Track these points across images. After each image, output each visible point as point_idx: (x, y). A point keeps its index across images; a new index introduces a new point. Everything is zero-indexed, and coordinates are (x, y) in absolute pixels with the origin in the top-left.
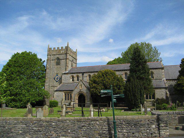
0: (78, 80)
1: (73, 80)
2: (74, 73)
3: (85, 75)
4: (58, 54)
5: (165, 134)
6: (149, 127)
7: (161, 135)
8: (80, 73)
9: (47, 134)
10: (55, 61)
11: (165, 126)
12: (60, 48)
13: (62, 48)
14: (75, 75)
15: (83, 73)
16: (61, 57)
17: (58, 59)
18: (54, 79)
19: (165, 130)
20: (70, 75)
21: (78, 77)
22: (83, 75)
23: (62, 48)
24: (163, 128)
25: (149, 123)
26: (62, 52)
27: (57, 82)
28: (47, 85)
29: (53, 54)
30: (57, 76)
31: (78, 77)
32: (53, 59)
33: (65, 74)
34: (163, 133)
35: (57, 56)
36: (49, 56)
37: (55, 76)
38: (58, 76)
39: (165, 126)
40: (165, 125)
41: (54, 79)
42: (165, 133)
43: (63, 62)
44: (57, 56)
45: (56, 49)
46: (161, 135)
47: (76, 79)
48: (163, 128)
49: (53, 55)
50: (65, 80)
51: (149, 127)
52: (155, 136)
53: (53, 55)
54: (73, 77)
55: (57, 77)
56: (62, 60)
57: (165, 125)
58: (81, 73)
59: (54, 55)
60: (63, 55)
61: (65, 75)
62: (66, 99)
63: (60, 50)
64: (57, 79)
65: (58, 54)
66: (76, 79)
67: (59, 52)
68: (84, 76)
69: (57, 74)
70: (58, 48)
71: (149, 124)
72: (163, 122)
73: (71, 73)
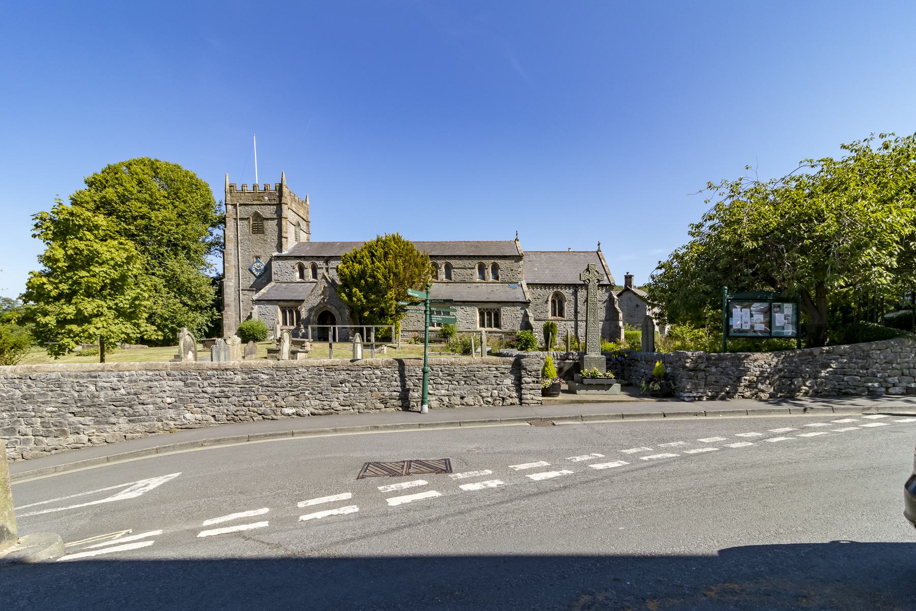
0: (315, 275)
1: (302, 276)
4: (255, 203)
5: (532, 399)
6: (499, 384)
7: (523, 401)
9: (246, 403)
11: (534, 382)
12: (262, 188)
14: (307, 264)
15: (327, 259)
17: (257, 216)
19: (532, 392)
20: (294, 263)
24: (528, 386)
25: (499, 375)
26: (267, 198)
28: (229, 286)
31: (314, 269)
34: (529, 396)
38: (259, 262)
39: (534, 382)
40: (534, 379)
42: (534, 397)
43: (271, 226)
46: (523, 401)
47: (309, 272)
48: (528, 386)
49: (241, 205)
51: (499, 384)
52: (511, 404)
53: (241, 205)
54: (301, 269)
55: (258, 264)
57: (534, 379)
60: (272, 207)
61: (280, 262)
62: (285, 323)
66: (309, 272)
69: (257, 257)
71: (498, 377)
72: (531, 372)
73: (296, 257)
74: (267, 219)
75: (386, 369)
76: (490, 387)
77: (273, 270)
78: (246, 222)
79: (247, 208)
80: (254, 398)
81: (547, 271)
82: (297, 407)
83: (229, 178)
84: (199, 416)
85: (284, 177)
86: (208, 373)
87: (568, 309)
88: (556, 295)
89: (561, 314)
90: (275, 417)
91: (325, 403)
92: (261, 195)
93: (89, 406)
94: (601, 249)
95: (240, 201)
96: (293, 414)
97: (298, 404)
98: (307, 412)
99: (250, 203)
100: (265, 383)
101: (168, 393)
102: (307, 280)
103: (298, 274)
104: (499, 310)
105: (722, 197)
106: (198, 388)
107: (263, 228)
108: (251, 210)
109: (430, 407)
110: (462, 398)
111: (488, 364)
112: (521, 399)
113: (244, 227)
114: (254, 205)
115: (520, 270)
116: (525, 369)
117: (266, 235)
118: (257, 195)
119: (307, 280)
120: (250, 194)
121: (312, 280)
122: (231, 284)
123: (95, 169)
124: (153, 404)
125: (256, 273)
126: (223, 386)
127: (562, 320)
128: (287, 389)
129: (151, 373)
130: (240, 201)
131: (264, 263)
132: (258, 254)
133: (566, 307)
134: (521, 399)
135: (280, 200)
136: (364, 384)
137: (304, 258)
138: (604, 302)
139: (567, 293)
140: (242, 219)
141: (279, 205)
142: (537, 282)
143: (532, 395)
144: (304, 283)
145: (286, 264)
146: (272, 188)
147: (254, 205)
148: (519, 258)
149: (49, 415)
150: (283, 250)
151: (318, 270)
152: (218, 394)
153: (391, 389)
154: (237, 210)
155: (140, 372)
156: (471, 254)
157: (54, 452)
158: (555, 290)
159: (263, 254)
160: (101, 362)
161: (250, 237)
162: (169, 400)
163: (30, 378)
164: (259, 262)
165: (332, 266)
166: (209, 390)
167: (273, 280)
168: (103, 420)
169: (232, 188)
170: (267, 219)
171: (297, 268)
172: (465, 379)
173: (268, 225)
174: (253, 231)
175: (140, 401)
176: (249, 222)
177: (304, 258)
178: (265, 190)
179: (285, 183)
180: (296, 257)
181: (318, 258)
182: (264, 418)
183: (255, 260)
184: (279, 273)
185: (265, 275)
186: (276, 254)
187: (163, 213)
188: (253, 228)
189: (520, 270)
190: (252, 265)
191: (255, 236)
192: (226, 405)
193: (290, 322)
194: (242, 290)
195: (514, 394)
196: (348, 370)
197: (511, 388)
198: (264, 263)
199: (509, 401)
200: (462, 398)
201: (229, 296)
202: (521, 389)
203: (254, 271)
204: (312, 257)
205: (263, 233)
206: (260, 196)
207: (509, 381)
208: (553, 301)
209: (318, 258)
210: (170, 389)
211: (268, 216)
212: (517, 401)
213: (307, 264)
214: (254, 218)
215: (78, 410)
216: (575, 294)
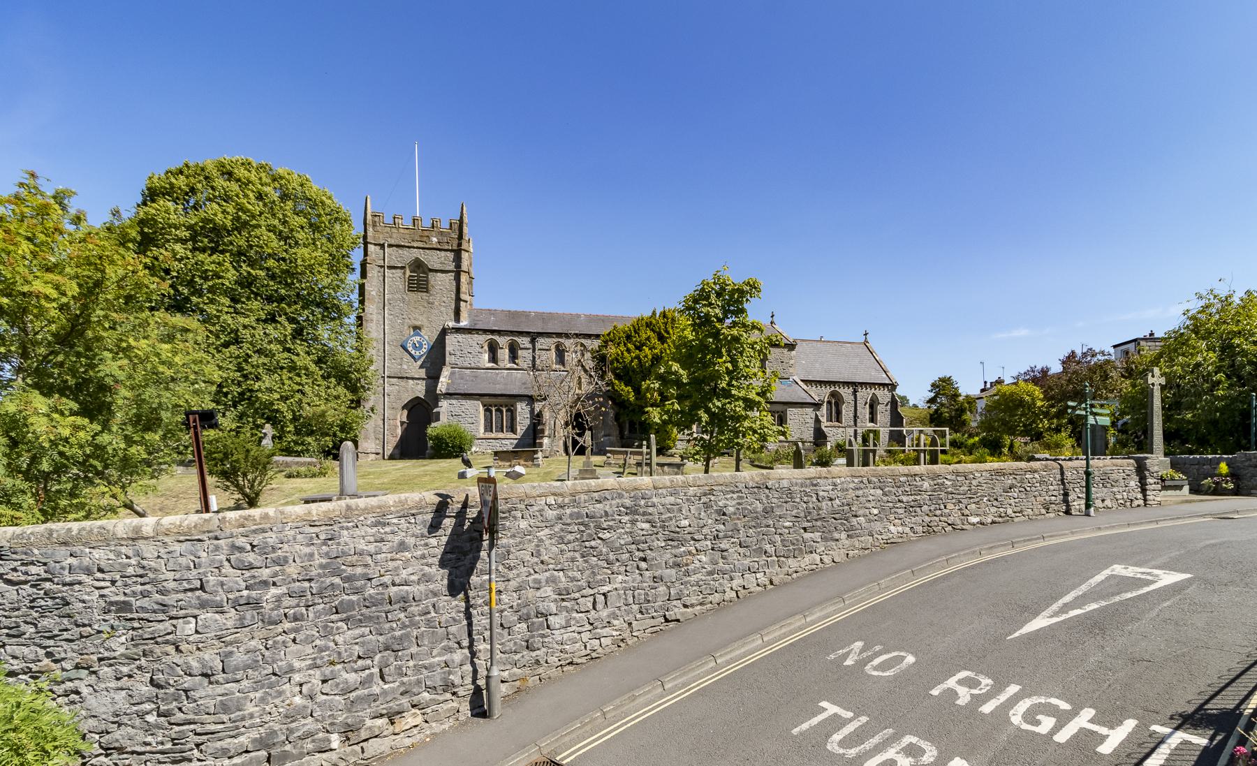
0: (514, 356)
1: (494, 359)
3: (542, 342)
4: (415, 244)
12: (428, 224)
14: (503, 341)
15: (534, 337)
16: (434, 260)
17: (418, 266)
20: (483, 339)
21: (561, 353)
22: (533, 341)
26: (435, 240)
29: (393, 242)
32: (392, 264)
35: (416, 254)
38: (420, 336)
41: (404, 348)
43: (442, 283)
44: (416, 254)
47: (504, 354)
54: (493, 349)
61: (460, 337)
67: (425, 239)
68: (538, 346)
69: (416, 328)
74: (437, 271)
75: (1045, 473)
76: (1121, 489)
77: (448, 349)
78: (399, 273)
79: (400, 252)
80: (942, 507)
81: (817, 365)
82: (980, 515)
83: (372, 204)
84: (900, 529)
85: (464, 212)
86: (902, 479)
87: (847, 412)
88: (833, 394)
89: (839, 420)
90: (964, 527)
91: (1001, 510)
92: (426, 233)
93: (816, 520)
94: (868, 340)
95: (389, 240)
96: (978, 523)
97: (980, 512)
98: (989, 520)
99: (407, 244)
100: (950, 489)
101: (873, 504)
102: (501, 365)
103: (486, 356)
104: (785, 413)
105: (1195, 306)
106: (894, 497)
107: (427, 284)
108: (409, 256)
109: (1097, 509)
110: (1103, 501)
111: (1117, 466)
112: (1145, 500)
113: (396, 280)
114: (414, 247)
115: (792, 362)
116: (1148, 470)
117: (431, 295)
118: (421, 235)
119: (501, 365)
120: (406, 231)
121: (509, 366)
123: (156, 170)
124: (864, 516)
125: (413, 352)
126: (915, 494)
127: (839, 427)
128: (967, 496)
129: (856, 480)
130: (389, 240)
131: (427, 337)
132: (418, 323)
133: (844, 411)
134: (1145, 500)
135: (460, 245)
136: (1028, 489)
137: (499, 332)
138: (887, 405)
139: (846, 393)
140: (390, 267)
141: (458, 253)
142: (811, 378)
143: (1155, 495)
145: (470, 340)
146: (445, 225)
147: (414, 247)
148: (791, 347)
149: (787, 531)
150: (462, 319)
151: (520, 352)
152: (912, 503)
153: (1050, 493)
154: (384, 253)
155: (848, 479)
156: (494, 328)
157: (795, 575)
158: (833, 389)
159: (425, 323)
160: (863, 466)
162: (875, 511)
163: (767, 488)
164: (420, 336)
165: (541, 347)
166: (905, 499)
167: (447, 363)
168: (828, 536)
169: (377, 219)
170: (437, 271)
171: (486, 348)
172: (1102, 482)
173: (435, 281)
174: (409, 287)
175: (854, 513)
176: (404, 273)
177: (499, 332)
178: (433, 227)
179: (466, 220)
180: (485, 331)
181: (521, 333)
182: (954, 528)
183: (412, 333)
184: (458, 353)
186: (451, 324)
187: (303, 252)
188: (409, 283)
189: (792, 362)
190: (408, 339)
192: (921, 516)
193: (496, 427)
194: (389, 377)
195: (1140, 496)
196: (1014, 474)
197: (1136, 490)
198: (427, 337)
199: (1136, 503)
200: (1103, 501)
202: (1146, 490)
203: (410, 349)
204: (511, 332)
205: (427, 292)
206: (424, 237)
207: (1134, 483)
208: (829, 403)
209: (521, 333)
210: (873, 498)
211: (437, 267)
212: (1141, 502)
213: (503, 341)
214: (412, 267)
215: (809, 524)
216: (855, 392)
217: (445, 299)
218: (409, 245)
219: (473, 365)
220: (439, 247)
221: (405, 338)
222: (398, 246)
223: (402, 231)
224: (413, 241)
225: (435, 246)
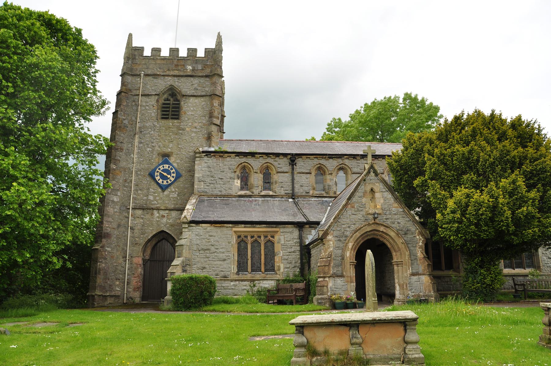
2: (252, 154)
8: (277, 155)
10: (158, 101)
12: (183, 53)
13: (192, 52)
15: (293, 158)
18: (152, 175)
23: (192, 52)
26: (190, 68)
27: (163, 188)
28: (113, 201)
30: (166, 162)
33: (208, 153)
35: (170, 81)
36: (129, 79)
37: (155, 165)
44: (170, 81)
45: (165, 53)
49: (146, 75)
50: (208, 180)
53: (146, 75)
55: (166, 166)
56: (192, 99)
58: (285, 155)
59: (155, 76)
63: (183, 59)
64: (163, 177)
65: (176, 73)
66: (257, 179)
69: (165, 157)
70: (174, 51)
79: (155, 80)
102: (256, 191)
108: (162, 84)
114: (168, 76)
122: (116, 199)
125: (160, 181)
130: (146, 71)
144: (250, 196)
161: (156, 124)
167: (196, 191)
173: (188, 106)
180: (239, 154)
185: (176, 184)
191: (164, 121)
201: (110, 219)
203: (157, 178)
217: (196, 125)
218: (165, 74)
219: (224, 193)
220: (193, 74)
221: (153, 167)
222: (155, 76)
223: (158, 62)
224: (169, 70)
225: (189, 74)
